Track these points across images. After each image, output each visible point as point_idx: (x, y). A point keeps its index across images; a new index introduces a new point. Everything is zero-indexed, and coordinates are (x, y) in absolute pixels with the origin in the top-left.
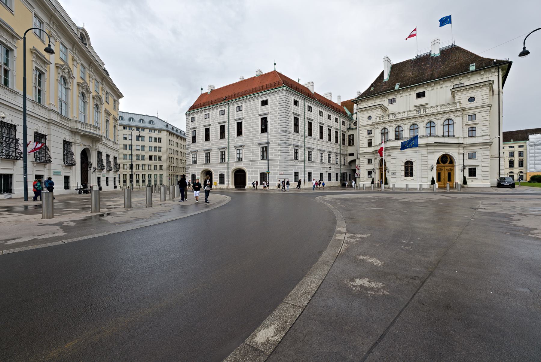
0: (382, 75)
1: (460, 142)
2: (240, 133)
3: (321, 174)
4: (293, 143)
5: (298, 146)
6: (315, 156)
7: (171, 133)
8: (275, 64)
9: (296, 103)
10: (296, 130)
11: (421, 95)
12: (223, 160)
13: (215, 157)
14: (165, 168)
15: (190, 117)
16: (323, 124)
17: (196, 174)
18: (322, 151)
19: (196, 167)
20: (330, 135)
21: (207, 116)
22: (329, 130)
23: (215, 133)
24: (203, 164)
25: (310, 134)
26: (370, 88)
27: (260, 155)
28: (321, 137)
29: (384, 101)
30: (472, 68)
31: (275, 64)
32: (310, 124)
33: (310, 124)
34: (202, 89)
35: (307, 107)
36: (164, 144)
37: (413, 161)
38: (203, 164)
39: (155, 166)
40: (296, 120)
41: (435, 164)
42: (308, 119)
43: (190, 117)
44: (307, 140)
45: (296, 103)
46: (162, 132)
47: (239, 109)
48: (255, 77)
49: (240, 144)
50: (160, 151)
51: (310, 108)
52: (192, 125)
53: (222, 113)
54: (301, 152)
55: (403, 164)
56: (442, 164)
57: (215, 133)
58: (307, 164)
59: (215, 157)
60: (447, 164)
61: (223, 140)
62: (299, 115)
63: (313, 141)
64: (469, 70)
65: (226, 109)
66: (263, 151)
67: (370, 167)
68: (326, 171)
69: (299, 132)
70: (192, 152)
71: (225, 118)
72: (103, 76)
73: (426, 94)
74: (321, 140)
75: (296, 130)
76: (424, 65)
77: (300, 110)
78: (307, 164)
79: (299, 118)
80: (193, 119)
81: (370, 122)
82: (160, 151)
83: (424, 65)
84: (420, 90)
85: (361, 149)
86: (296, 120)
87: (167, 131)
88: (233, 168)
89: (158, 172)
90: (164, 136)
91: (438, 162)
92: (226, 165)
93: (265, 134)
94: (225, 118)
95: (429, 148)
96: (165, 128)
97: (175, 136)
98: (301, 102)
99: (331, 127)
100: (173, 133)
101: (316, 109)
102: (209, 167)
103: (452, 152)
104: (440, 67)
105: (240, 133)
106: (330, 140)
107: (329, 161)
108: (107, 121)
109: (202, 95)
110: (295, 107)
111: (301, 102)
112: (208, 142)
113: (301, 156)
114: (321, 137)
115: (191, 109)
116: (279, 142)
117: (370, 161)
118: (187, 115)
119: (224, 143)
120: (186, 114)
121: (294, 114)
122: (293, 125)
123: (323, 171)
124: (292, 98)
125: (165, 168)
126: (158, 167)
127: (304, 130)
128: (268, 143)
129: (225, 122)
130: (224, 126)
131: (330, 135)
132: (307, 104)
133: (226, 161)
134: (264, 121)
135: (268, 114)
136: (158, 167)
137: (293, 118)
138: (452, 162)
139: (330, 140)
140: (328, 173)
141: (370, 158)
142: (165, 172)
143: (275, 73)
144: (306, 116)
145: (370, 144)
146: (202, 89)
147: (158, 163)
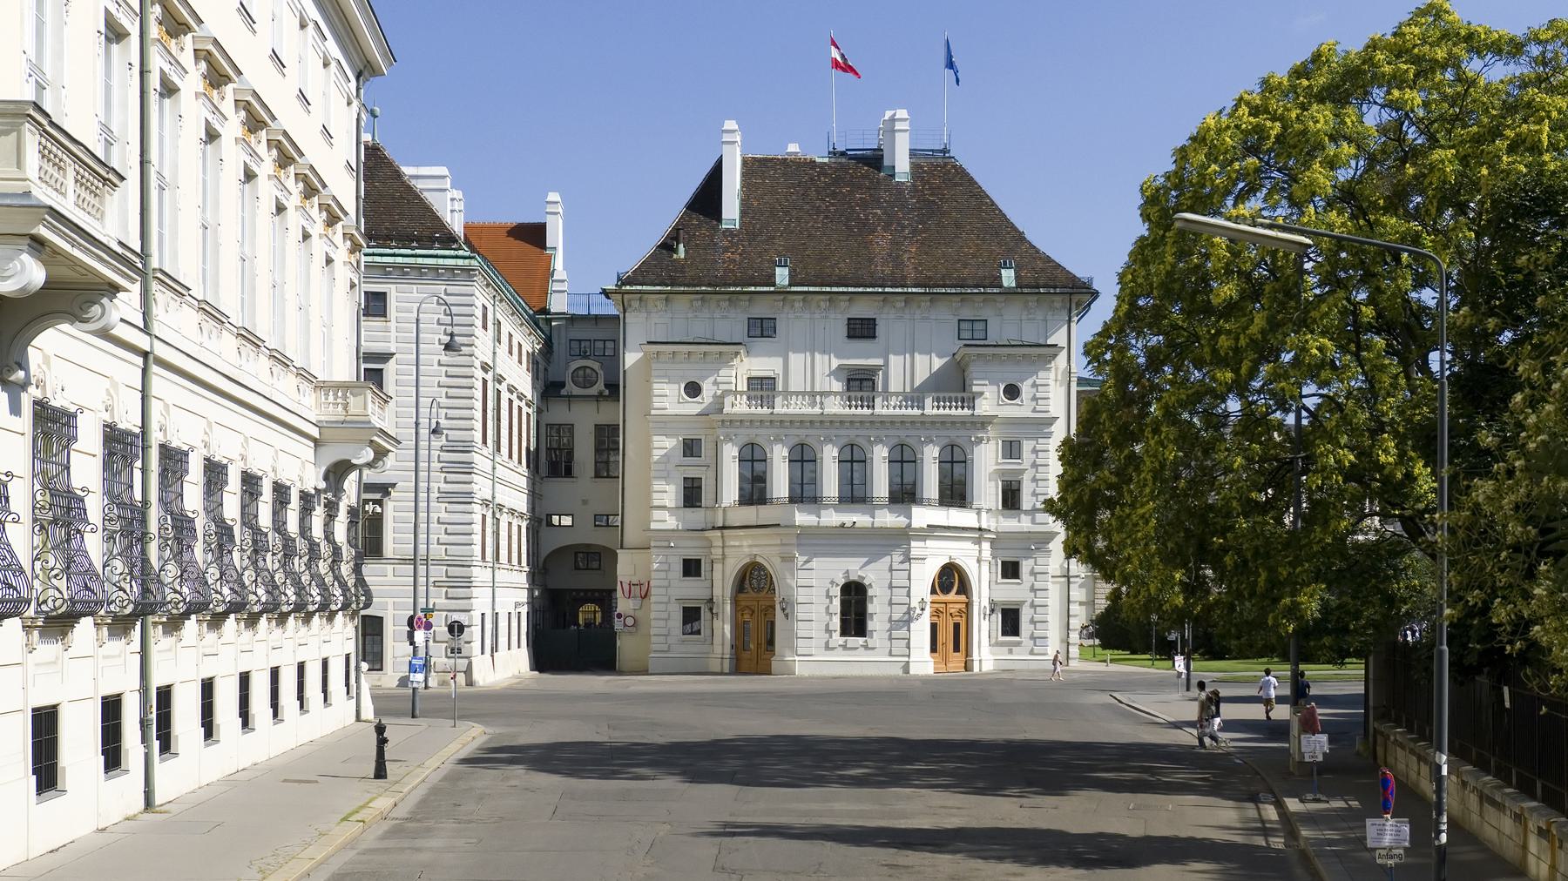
0: (707, 198)
1: (984, 526)
11: (862, 330)
26: (667, 246)
29: (731, 322)
30: (1008, 277)
37: (866, 582)
41: (929, 598)
55: (837, 591)
56: (942, 597)
60: (952, 596)
64: (1001, 286)
67: (693, 589)
73: (880, 330)
76: (864, 205)
81: (693, 407)
83: (864, 205)
84: (862, 310)
85: (656, 514)
91: (933, 591)
95: (913, 544)
103: (966, 555)
104: (915, 231)
117: (691, 568)
138: (964, 588)
141: (692, 554)
145: (692, 495)
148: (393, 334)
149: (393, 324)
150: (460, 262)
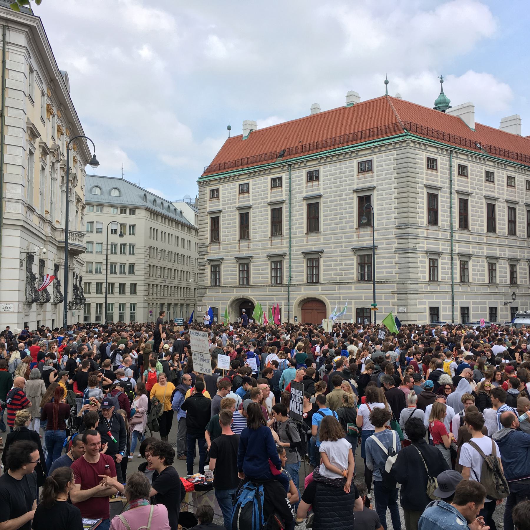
2: (313, 225)
3: (493, 311)
4: (425, 245)
5: (439, 254)
6: (478, 270)
7: (153, 213)
8: (386, 83)
9: (431, 164)
10: (433, 220)
12: (277, 279)
13: (260, 272)
14: (141, 289)
15: (208, 190)
16: (496, 199)
17: (220, 307)
18: (492, 262)
19: (220, 292)
20: (512, 222)
21: (244, 190)
22: (512, 210)
23: (261, 223)
24: (235, 287)
25: (464, 223)
27: (355, 272)
28: (491, 227)
31: (386, 83)
32: (464, 205)
33: (464, 205)
34: (229, 128)
35: (455, 169)
36: (140, 239)
38: (235, 287)
39: (122, 286)
40: (433, 199)
42: (458, 192)
43: (208, 190)
44: (456, 236)
45: (431, 164)
46: (137, 212)
47: (313, 177)
48: (343, 108)
49: (313, 249)
50: (132, 253)
51: (462, 170)
52: (211, 206)
53: (276, 183)
54: (443, 264)
57: (261, 223)
58: (458, 289)
59: (260, 272)
61: (277, 240)
62: (438, 189)
63: (471, 238)
65: (285, 176)
66: (361, 265)
68: (506, 303)
69: (440, 223)
70: (211, 261)
71: (282, 194)
72: (77, 139)
74: (492, 235)
75: (433, 220)
77: (439, 178)
78: (458, 289)
79: (440, 194)
80: (215, 194)
82: (132, 253)
86: (433, 199)
87: (147, 209)
88: (299, 298)
89: (127, 299)
90: (141, 220)
92: (282, 292)
93: (366, 231)
94: (282, 194)
96: (141, 203)
97: (160, 218)
98: (442, 160)
99: (516, 203)
100: (161, 212)
101: (477, 169)
102: (248, 293)
105: (313, 225)
106: (512, 232)
107: (513, 281)
108: (77, 212)
109: (230, 142)
110: (430, 172)
111: (442, 160)
112: (244, 243)
113: (443, 273)
114: (491, 227)
115: (209, 171)
116: (396, 245)
118: (201, 183)
119: (279, 246)
120: (199, 183)
121: (427, 186)
122: (425, 210)
123: (498, 303)
124: (421, 156)
125: (141, 289)
126: (128, 288)
127: (451, 217)
128: (374, 248)
129: (282, 202)
130: (280, 209)
131: (512, 222)
132: (456, 162)
133: (285, 281)
134: (365, 204)
135: (372, 189)
136: (128, 288)
137: (425, 196)
139: (512, 232)
140: (509, 306)
142: (139, 298)
143: (384, 102)
144: (456, 187)
146: (229, 128)
147: (128, 279)
148: (375, 178)
149: (375, 173)
150: (401, 138)
